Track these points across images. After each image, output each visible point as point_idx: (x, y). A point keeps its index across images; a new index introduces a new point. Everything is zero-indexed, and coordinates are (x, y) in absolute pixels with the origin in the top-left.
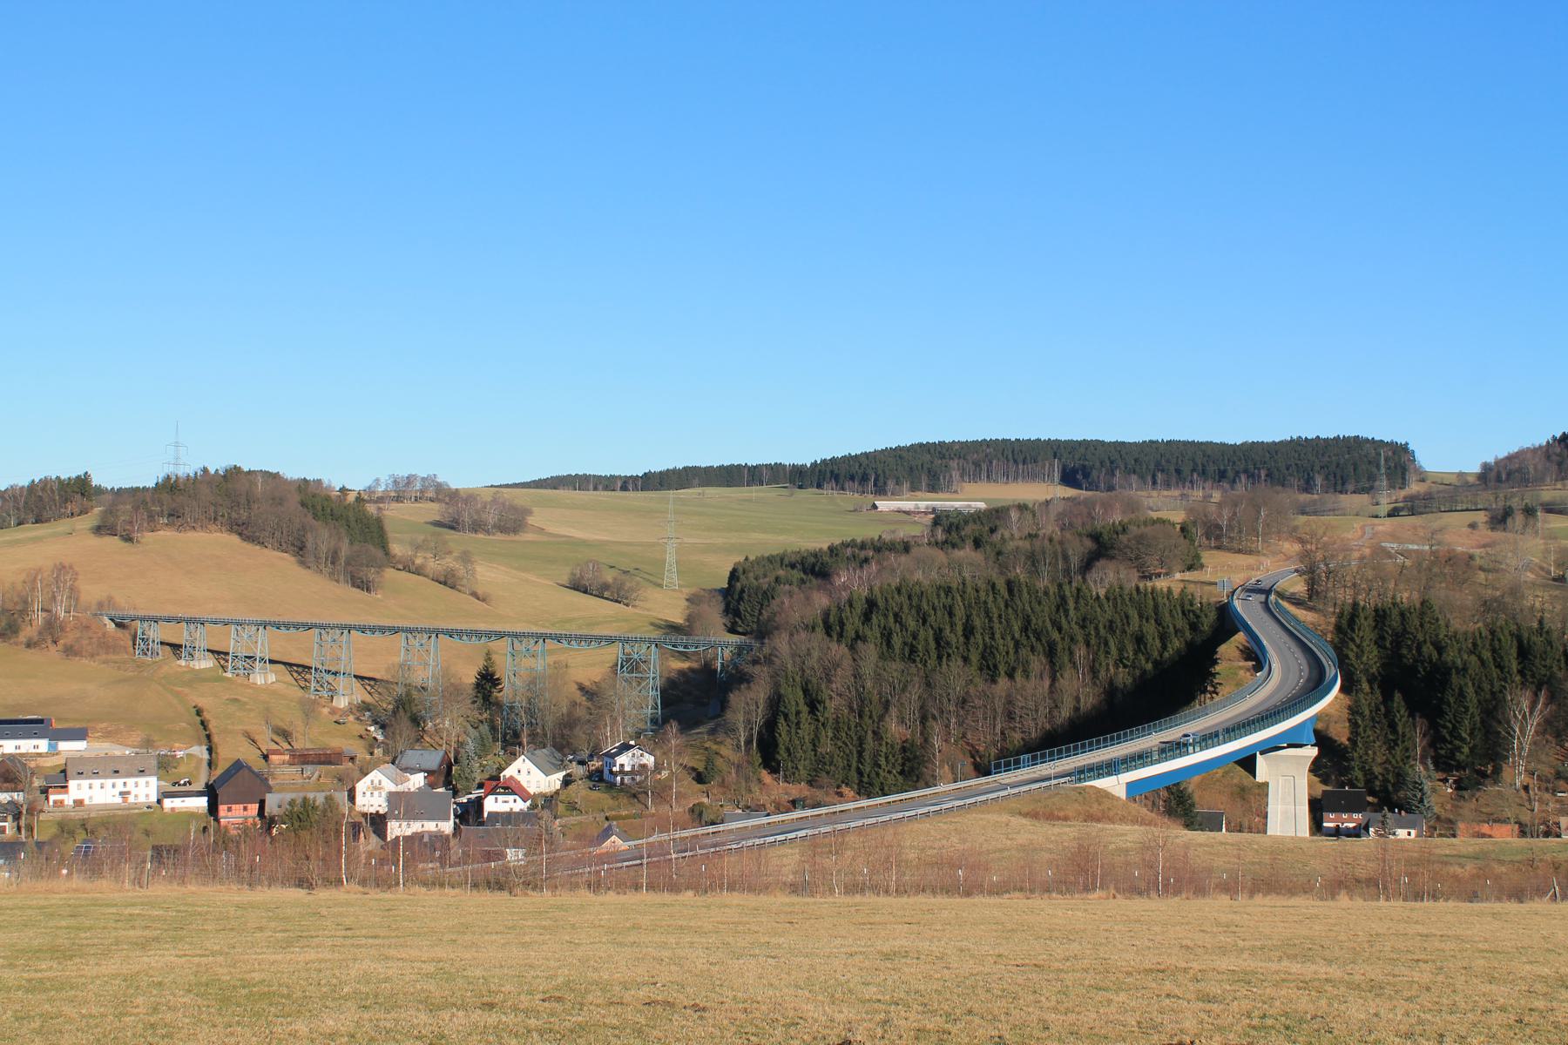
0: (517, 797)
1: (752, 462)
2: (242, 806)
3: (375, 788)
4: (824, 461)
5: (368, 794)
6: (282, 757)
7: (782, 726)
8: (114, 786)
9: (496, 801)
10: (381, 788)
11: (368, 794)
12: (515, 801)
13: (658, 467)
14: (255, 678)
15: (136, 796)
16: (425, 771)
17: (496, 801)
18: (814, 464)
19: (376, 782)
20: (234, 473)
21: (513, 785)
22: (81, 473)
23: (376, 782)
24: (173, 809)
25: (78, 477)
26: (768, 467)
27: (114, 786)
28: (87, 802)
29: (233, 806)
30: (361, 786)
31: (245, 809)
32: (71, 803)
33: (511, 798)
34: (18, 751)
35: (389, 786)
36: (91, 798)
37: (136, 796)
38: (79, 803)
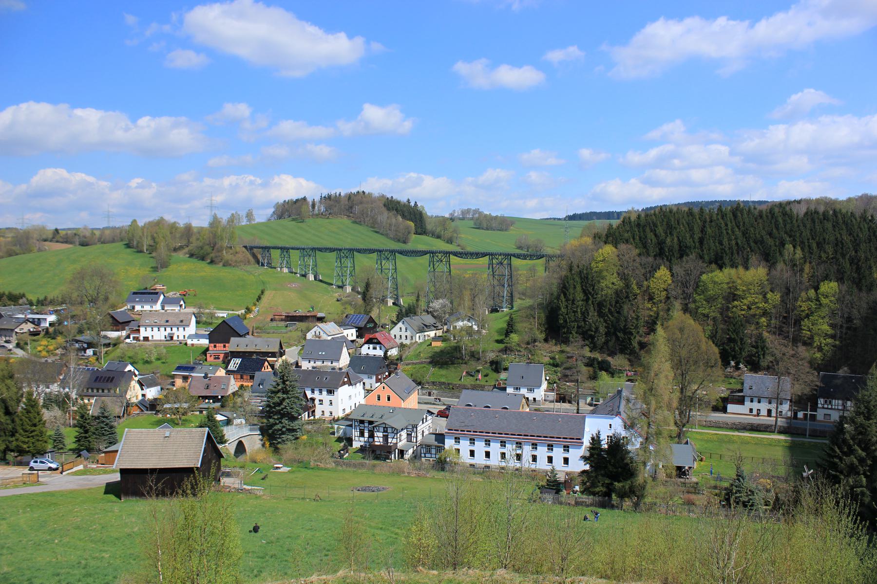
0: (382, 347)
2: (222, 345)
8: (165, 330)
9: (369, 348)
15: (178, 336)
16: (356, 328)
17: (369, 348)
24: (193, 345)
27: (165, 330)
28: (150, 338)
29: (217, 345)
31: (225, 346)
32: (142, 338)
33: (378, 347)
34: (142, 309)
36: (152, 336)
37: (178, 336)
38: (146, 339)
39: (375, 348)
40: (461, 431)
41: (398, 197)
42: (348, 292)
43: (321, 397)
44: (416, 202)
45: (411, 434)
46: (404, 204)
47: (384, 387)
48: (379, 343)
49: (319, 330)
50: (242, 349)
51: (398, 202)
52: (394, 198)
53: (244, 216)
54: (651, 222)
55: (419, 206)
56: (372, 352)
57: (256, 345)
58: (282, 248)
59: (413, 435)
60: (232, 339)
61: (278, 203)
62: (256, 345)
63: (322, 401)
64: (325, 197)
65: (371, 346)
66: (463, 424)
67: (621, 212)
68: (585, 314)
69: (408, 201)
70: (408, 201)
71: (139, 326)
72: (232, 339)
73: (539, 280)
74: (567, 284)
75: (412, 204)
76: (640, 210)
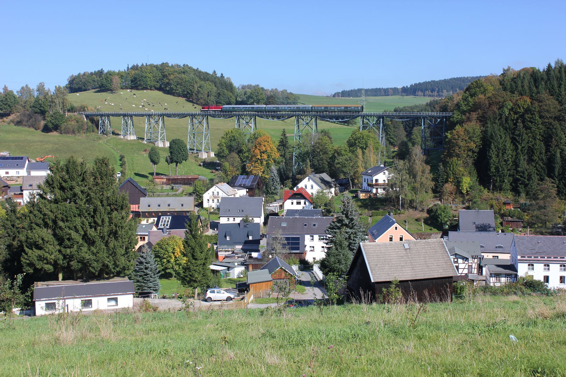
1: (385, 87)
3: (215, 197)
4: (415, 84)
5: (211, 201)
6: (162, 180)
7: (493, 153)
9: (292, 203)
10: (219, 197)
11: (211, 201)
12: (305, 203)
13: (348, 89)
14: (158, 144)
16: (247, 188)
17: (292, 203)
18: (411, 86)
19: (216, 193)
20: (164, 65)
21: (304, 193)
22: (100, 69)
23: (216, 193)
25: (98, 71)
26: (391, 89)
30: (206, 196)
33: (302, 201)
34: (7, 175)
35: (222, 195)
39: (299, 203)
40: (528, 257)
41: (203, 69)
42: (204, 158)
43: (312, 244)
44: (222, 74)
45: (472, 266)
46: (212, 76)
47: (396, 228)
48: (304, 198)
49: (218, 190)
50: (154, 209)
51: (207, 74)
52: (200, 69)
53: (36, 88)
54: (555, 76)
55: (225, 78)
56: (296, 207)
57: (169, 205)
58: (124, 115)
59: (473, 267)
60: (142, 199)
61: (73, 75)
62: (169, 205)
63: (313, 247)
64: (131, 68)
65: (295, 201)
66: (535, 252)
67: (387, 89)
68: (516, 164)
69: (215, 72)
70: (215, 72)
71: (22, 191)
72: (142, 199)
73: (482, 128)
74: (493, 134)
75: (219, 75)
76: (409, 86)
